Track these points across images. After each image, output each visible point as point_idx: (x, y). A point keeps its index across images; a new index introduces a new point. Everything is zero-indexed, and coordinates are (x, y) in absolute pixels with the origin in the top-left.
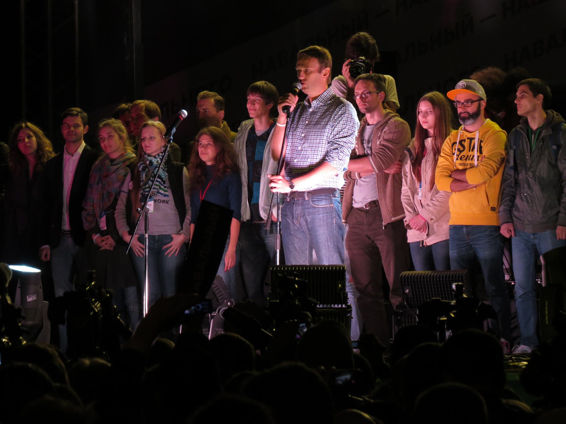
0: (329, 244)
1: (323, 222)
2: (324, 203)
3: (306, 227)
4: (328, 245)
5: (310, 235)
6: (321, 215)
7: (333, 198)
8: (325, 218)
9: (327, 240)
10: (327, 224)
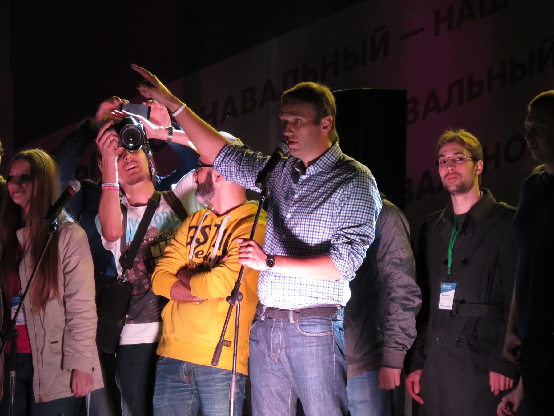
0: (326, 393)
1: (317, 358)
2: (318, 331)
3: (288, 365)
4: (324, 396)
5: (295, 378)
6: (313, 348)
7: (333, 323)
8: (320, 354)
9: (323, 389)
10: (323, 362)
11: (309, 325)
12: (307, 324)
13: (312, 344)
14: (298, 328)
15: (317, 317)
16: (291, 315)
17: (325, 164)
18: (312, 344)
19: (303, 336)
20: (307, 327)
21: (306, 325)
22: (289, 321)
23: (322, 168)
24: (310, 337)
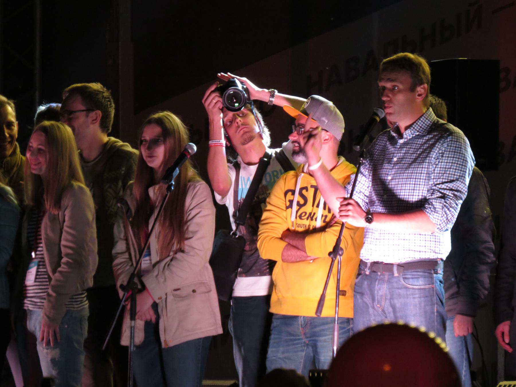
1: (420, 309)
7: (435, 275)
8: (423, 305)
11: (412, 278)
12: (410, 276)
13: (415, 296)
14: (402, 280)
15: (419, 270)
16: (395, 268)
17: (421, 127)
18: (415, 296)
19: (406, 288)
20: (411, 280)
21: (409, 278)
22: (393, 274)
23: (418, 131)
24: (413, 289)
